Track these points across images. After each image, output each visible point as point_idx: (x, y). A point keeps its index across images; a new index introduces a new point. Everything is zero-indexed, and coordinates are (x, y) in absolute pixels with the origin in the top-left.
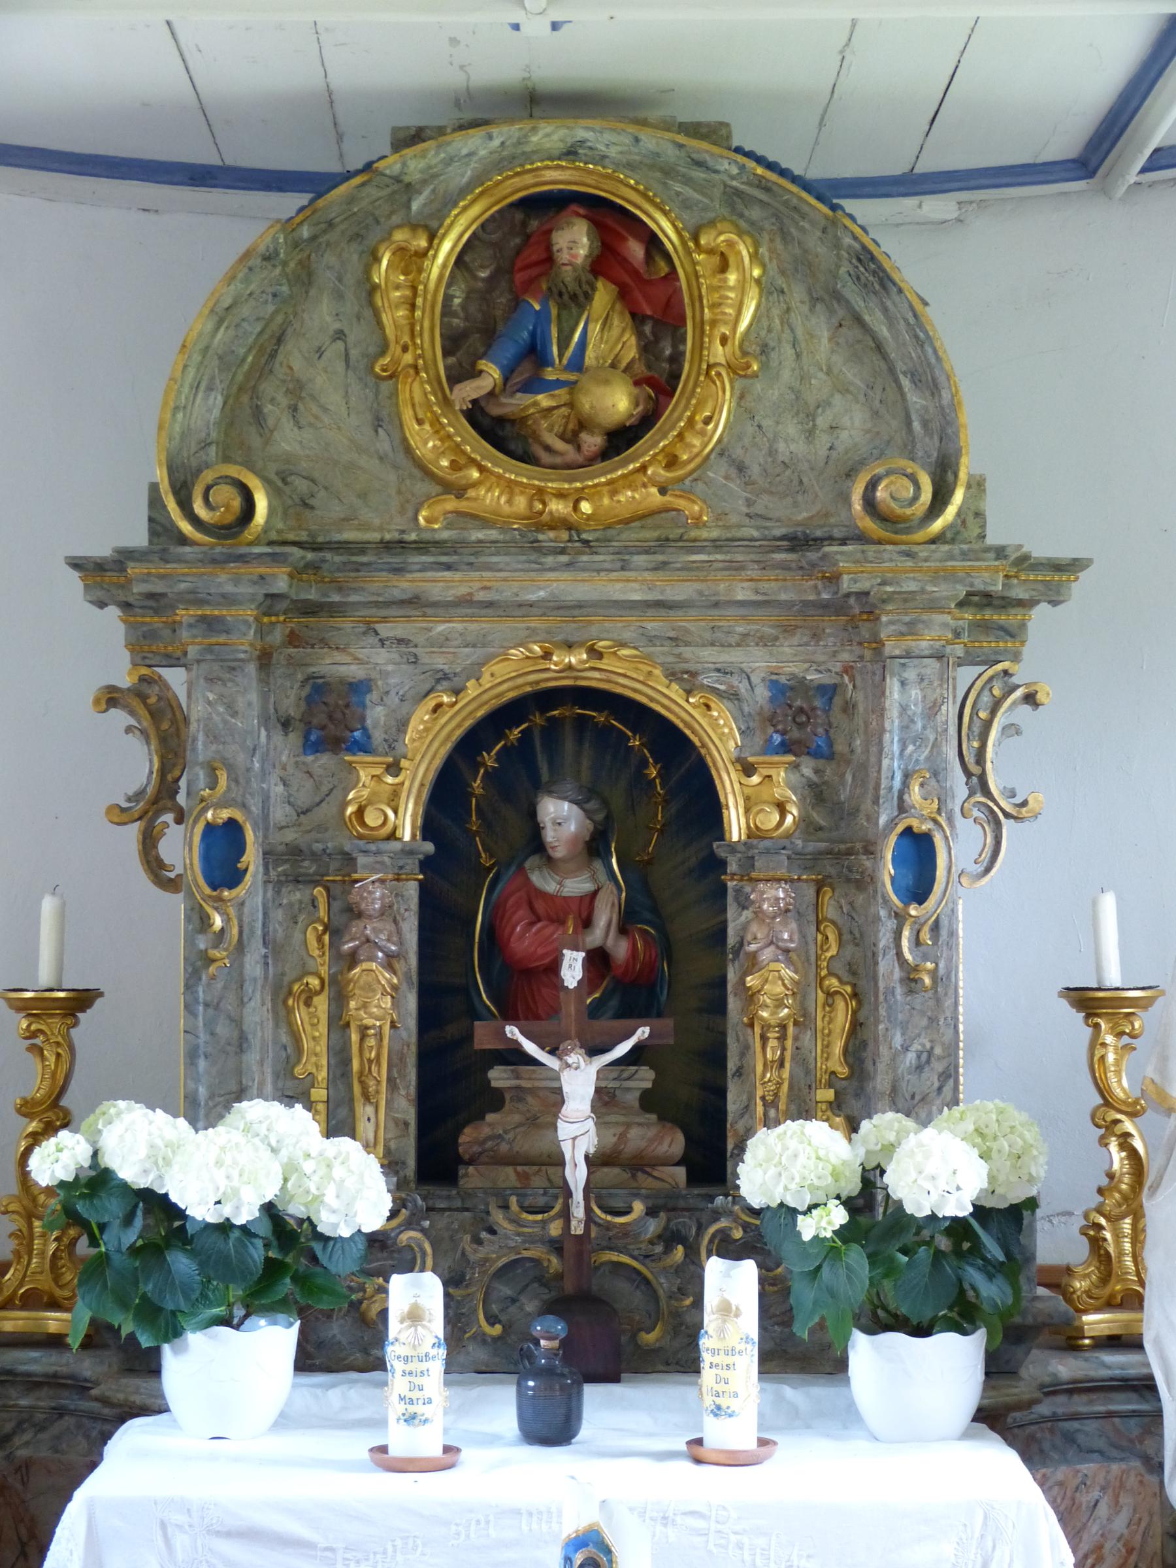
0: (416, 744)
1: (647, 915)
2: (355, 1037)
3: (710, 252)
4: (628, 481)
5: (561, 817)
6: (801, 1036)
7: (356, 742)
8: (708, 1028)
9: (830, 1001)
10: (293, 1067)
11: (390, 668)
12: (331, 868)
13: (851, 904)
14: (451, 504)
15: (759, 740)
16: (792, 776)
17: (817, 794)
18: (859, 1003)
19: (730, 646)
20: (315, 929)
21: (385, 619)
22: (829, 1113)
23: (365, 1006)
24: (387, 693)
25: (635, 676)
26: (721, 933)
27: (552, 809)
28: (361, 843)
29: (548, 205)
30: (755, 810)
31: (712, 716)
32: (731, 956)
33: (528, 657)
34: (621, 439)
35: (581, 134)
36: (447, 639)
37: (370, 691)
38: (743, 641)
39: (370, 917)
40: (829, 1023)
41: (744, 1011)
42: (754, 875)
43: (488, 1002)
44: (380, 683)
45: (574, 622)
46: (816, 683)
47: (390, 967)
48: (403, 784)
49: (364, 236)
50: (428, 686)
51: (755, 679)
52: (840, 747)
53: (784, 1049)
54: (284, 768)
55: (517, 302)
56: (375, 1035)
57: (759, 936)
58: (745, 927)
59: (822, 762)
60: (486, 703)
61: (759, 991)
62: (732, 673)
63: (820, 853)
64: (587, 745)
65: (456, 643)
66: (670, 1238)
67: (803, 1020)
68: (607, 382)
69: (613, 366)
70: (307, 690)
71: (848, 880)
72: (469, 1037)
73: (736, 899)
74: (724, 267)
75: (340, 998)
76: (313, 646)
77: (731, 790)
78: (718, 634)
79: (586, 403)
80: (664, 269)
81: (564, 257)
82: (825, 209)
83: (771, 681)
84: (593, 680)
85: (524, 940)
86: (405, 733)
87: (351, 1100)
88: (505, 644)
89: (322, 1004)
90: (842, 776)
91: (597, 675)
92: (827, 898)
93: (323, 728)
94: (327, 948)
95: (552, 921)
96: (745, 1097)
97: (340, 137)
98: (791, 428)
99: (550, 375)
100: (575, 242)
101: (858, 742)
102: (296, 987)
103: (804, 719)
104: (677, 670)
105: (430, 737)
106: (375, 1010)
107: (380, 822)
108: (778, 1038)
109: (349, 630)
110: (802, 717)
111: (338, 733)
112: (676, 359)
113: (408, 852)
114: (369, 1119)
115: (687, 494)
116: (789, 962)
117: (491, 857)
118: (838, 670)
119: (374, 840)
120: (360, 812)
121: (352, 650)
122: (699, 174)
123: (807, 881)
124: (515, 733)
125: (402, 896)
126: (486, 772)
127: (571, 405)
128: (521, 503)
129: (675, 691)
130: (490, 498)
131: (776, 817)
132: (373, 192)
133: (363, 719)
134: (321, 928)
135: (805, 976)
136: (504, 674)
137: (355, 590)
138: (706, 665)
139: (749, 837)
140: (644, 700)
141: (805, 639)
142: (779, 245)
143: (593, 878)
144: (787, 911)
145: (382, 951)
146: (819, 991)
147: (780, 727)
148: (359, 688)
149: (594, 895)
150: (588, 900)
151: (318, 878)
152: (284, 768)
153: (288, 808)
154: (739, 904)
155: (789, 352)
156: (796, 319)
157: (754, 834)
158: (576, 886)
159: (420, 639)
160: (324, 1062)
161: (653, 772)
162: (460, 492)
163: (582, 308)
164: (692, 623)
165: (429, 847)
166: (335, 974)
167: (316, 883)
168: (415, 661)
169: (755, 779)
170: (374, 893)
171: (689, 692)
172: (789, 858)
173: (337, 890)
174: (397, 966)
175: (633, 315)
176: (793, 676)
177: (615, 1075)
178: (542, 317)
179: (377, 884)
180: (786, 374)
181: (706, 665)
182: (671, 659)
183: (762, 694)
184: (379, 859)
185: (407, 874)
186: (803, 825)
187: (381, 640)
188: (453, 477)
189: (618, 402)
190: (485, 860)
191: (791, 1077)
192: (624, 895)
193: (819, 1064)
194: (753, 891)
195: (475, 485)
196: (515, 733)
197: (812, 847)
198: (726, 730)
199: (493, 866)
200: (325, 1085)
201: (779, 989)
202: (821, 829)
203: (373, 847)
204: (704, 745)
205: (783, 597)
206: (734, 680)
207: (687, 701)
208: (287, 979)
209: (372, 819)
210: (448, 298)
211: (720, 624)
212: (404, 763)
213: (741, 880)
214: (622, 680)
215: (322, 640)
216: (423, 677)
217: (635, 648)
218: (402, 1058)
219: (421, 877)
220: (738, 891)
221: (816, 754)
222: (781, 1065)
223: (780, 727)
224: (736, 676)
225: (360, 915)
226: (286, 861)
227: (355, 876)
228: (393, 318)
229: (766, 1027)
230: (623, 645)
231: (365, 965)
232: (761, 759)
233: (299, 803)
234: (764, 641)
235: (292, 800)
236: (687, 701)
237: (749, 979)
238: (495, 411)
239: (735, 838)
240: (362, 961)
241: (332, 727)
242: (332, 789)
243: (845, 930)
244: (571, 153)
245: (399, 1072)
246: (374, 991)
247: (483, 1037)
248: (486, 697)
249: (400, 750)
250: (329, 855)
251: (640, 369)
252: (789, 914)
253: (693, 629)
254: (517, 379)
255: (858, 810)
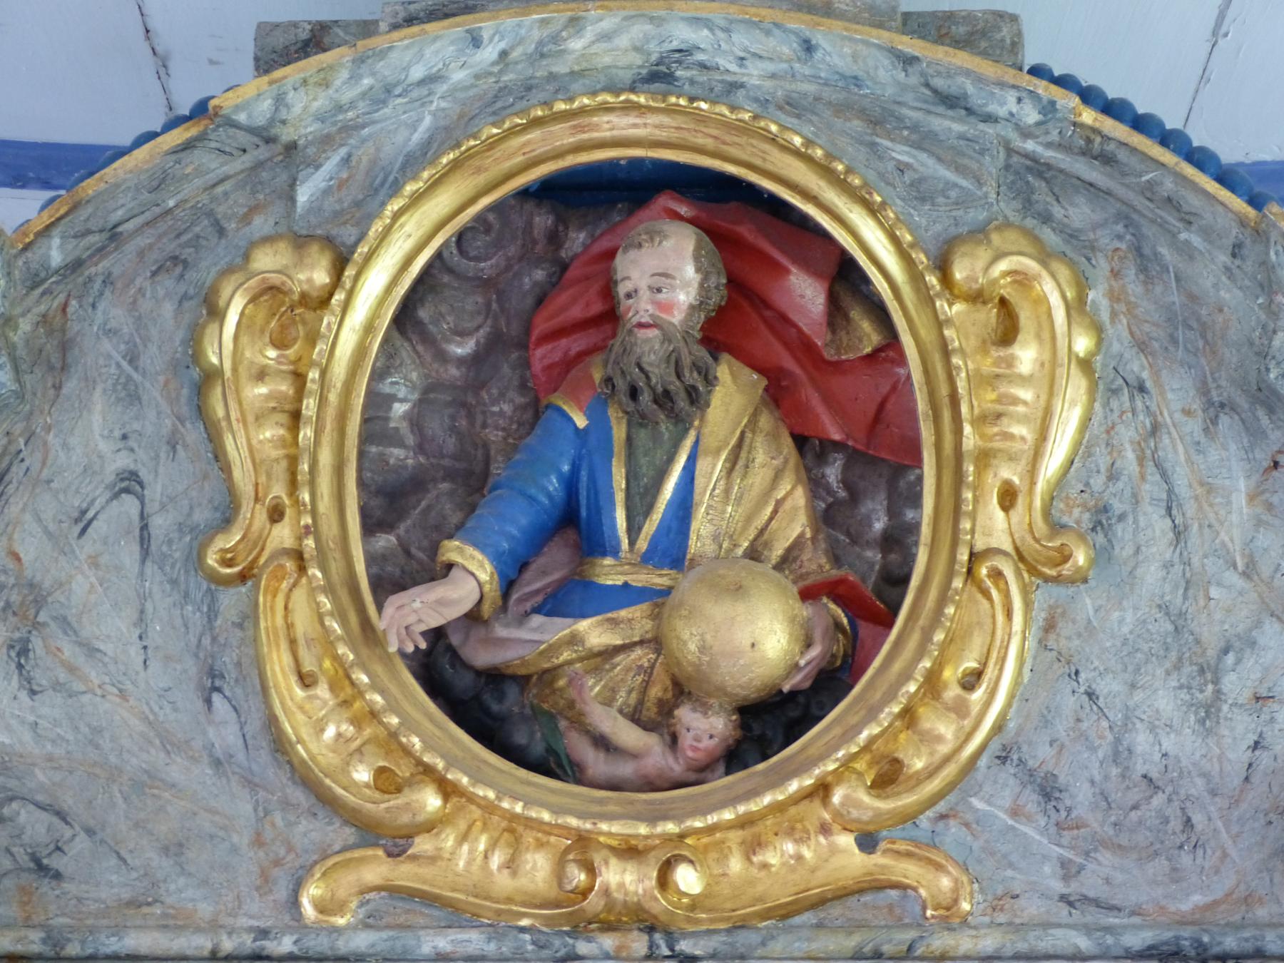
3: (977, 297)
4: (784, 817)
14: (377, 869)
29: (605, 195)
34: (772, 722)
35: (682, 34)
49: (187, 258)
55: (536, 411)
68: (738, 591)
69: (754, 554)
74: (1007, 333)
79: (689, 639)
80: (868, 336)
81: (641, 308)
82: (1238, 204)
97: (162, 63)
98: (1164, 700)
99: (609, 573)
100: (667, 274)
112: (899, 541)
115: (926, 851)
122: (949, 125)
127: (656, 643)
128: (538, 868)
130: (463, 857)
132: (208, 162)
142: (1133, 285)
155: (1161, 526)
156: (1174, 451)
162: (397, 841)
163: (681, 423)
175: (801, 441)
178: (591, 446)
180: (1151, 575)
188: (380, 807)
189: (764, 637)
195: (431, 826)
210: (377, 403)
228: (252, 443)
238: (482, 657)
244: (658, 76)
251: (816, 564)
254: (534, 583)
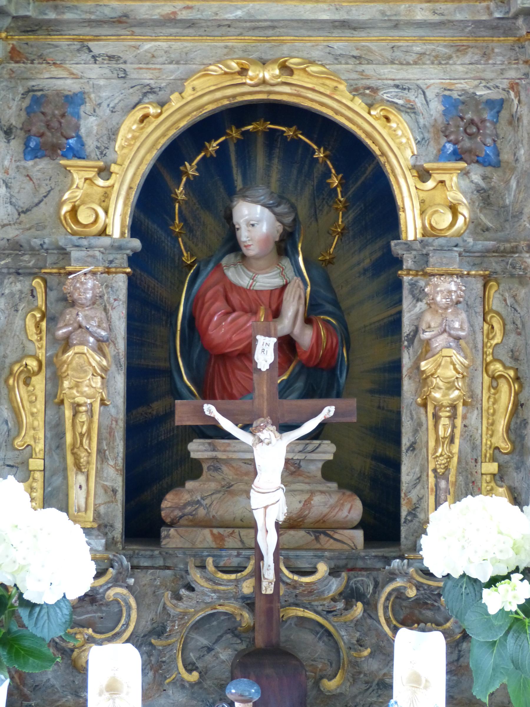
0: (125, 151)
1: (329, 307)
2: (68, 413)
5: (255, 219)
6: (469, 415)
7: (71, 148)
8: (379, 407)
9: (495, 384)
10: (14, 439)
11: (102, 82)
12: (49, 260)
13: (514, 297)
15: (433, 150)
16: (462, 182)
17: (485, 198)
18: (521, 386)
19: (408, 64)
20: (34, 316)
21: (97, 38)
22: (493, 484)
23: (77, 385)
24: (100, 104)
25: (322, 90)
26: (396, 323)
27: (246, 212)
28: (74, 238)
30: (430, 211)
31: (390, 127)
32: (406, 343)
33: (226, 73)
36: (153, 56)
37: (83, 102)
38: (420, 59)
39: (82, 305)
40: (494, 404)
41: (417, 392)
42: (429, 270)
43: (189, 384)
44: (93, 96)
45: (268, 41)
46: (485, 98)
47: (100, 351)
48: (113, 186)
50: (136, 99)
51: (430, 94)
52: (505, 156)
53: (454, 427)
54: (7, 172)
56: (86, 411)
57: (433, 325)
58: (420, 317)
59: (489, 169)
60: (188, 114)
61: (432, 375)
62: (409, 89)
63: (488, 251)
64: (276, 161)
65: (161, 60)
66: (351, 595)
67: (471, 401)
70: (27, 102)
71: (512, 276)
72: (170, 414)
73: (411, 292)
75: (55, 379)
76: (32, 63)
77: (407, 193)
78: (398, 54)
83: (445, 96)
84: (284, 94)
85: (220, 329)
86: (115, 140)
87: (65, 469)
88: (206, 61)
89: (39, 383)
90: (507, 182)
91: (287, 89)
92: (492, 292)
93: (42, 135)
94: (44, 333)
95: (246, 311)
96: (417, 469)
101: (522, 152)
102: (16, 368)
103: (474, 130)
104: (360, 85)
105: (138, 144)
106: (86, 389)
107: (92, 219)
108: (449, 417)
109: (65, 48)
110: (473, 129)
111: (55, 140)
113: (119, 248)
114: (80, 487)
116: (460, 349)
117: (192, 256)
118: (505, 86)
119: (86, 236)
120: (74, 211)
121: (68, 66)
123: (475, 276)
124: (213, 146)
125: (112, 287)
126: (188, 180)
129: (358, 105)
131: (449, 217)
133: (77, 128)
134: (38, 315)
135: (473, 361)
136: (203, 92)
137: (69, 8)
138: (386, 82)
139: (423, 236)
140: (329, 113)
141: (476, 58)
143: (282, 274)
144: (458, 303)
145: (93, 336)
146: (485, 375)
147: (452, 137)
148: (73, 100)
149: (283, 288)
150: (277, 293)
151: (36, 270)
152: (7, 172)
153: (10, 208)
154: (414, 296)
157: (430, 232)
158: (267, 281)
159: (129, 56)
160: (41, 435)
161: (335, 181)
164: (374, 43)
165: (136, 244)
166: (51, 357)
167: (35, 275)
168: (124, 76)
169: (430, 184)
170: (86, 283)
171: (370, 106)
172: (460, 255)
173: (53, 281)
174: (106, 350)
176: (465, 92)
177: (300, 448)
179: (89, 276)
181: (386, 82)
182: (355, 76)
183: (436, 107)
184: (91, 253)
185: (116, 268)
186: (471, 226)
187: (93, 57)
190: (187, 258)
191: (460, 451)
192: (309, 289)
193: (484, 441)
194: (427, 284)
196: (213, 146)
197: (481, 245)
198: (404, 140)
199: (194, 263)
200: (42, 456)
201: (450, 373)
202: (488, 229)
203: (85, 242)
204: (383, 154)
205: (459, 17)
206: (411, 96)
207: (369, 113)
208: (8, 361)
209: (85, 217)
211: (399, 44)
212: (114, 168)
213: (416, 275)
214: (311, 95)
215: (40, 57)
216: (131, 90)
217: (322, 65)
218: (111, 432)
219: (129, 270)
220: (413, 285)
221: (483, 162)
222: (452, 441)
223: (452, 137)
224: (412, 92)
225: (73, 304)
226: (8, 255)
227: (69, 268)
229: (438, 407)
230: (312, 62)
231: (77, 349)
232: (435, 165)
233: (20, 203)
234: (439, 60)
235: (13, 200)
236: (369, 113)
237: (423, 364)
239: (411, 237)
240: (75, 345)
241: (49, 134)
242: (49, 191)
243: (508, 321)
245: (108, 444)
246: (85, 371)
247: (183, 414)
248: (188, 109)
249: (111, 156)
250: (47, 250)
252: (459, 306)
253: (374, 48)
255: (521, 213)
